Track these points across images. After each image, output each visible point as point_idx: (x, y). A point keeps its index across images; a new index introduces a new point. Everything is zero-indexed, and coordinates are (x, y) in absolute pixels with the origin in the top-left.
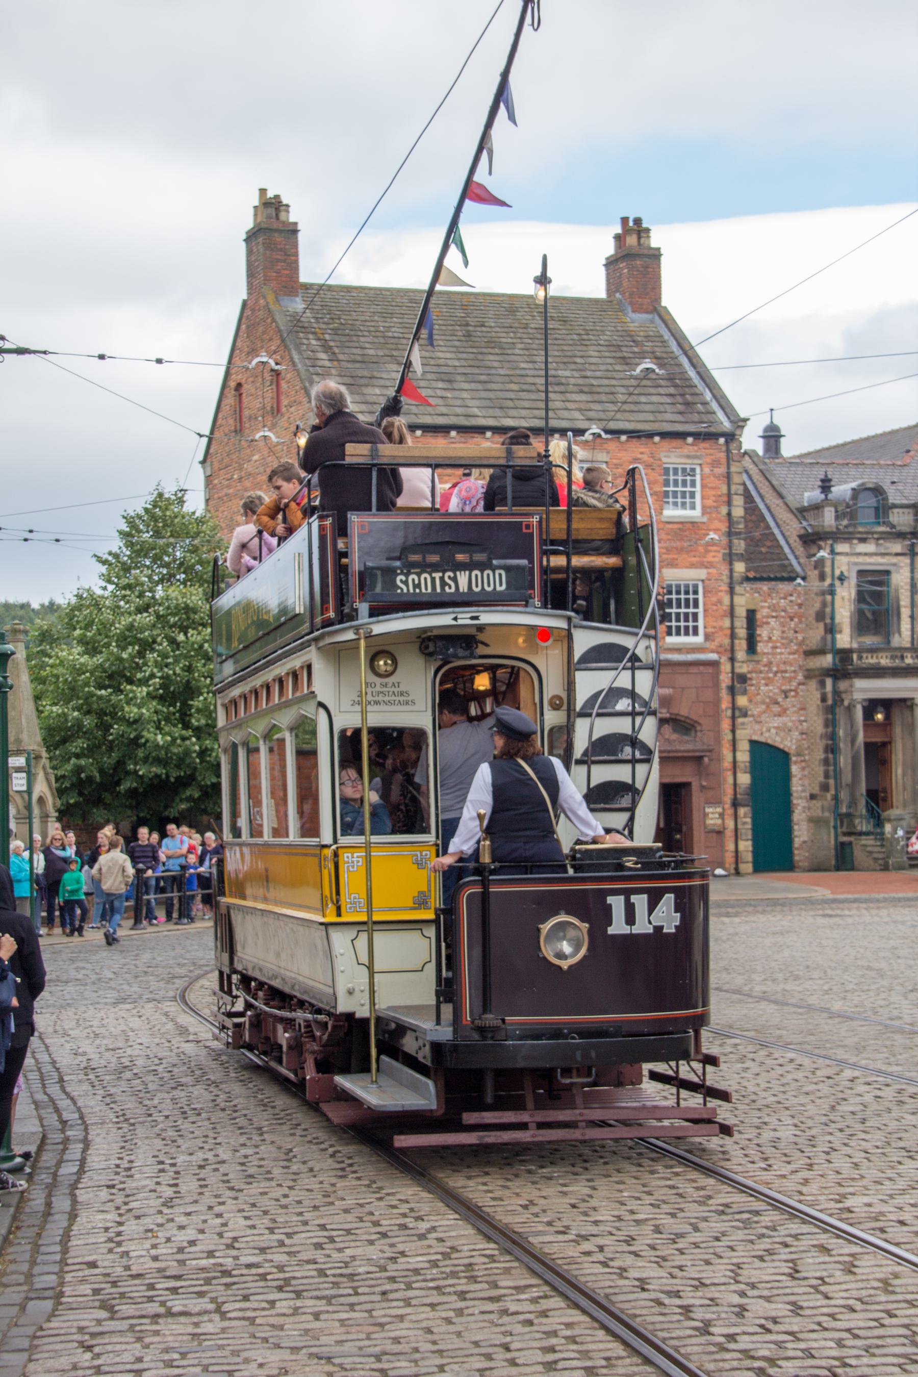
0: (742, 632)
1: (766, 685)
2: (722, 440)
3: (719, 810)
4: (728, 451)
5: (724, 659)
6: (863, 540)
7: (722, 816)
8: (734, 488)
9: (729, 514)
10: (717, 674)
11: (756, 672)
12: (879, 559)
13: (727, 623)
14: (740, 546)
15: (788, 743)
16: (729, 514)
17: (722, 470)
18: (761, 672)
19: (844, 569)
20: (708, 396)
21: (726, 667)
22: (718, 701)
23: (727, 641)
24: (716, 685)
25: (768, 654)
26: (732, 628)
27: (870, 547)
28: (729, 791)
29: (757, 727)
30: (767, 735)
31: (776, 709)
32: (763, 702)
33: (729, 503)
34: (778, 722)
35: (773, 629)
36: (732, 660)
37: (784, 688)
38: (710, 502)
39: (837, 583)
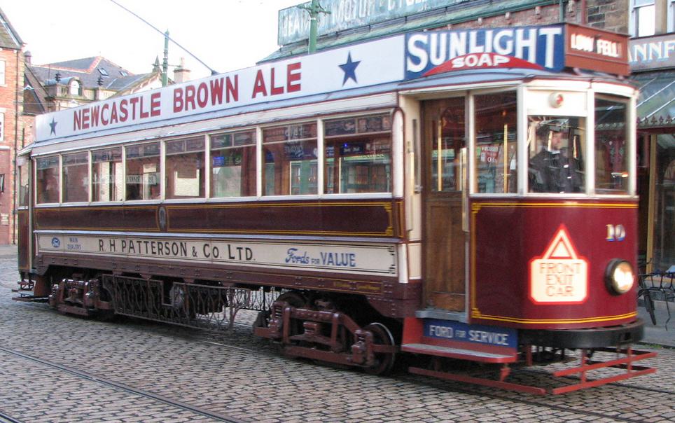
0: (20, 137)
2: (15, 51)
3: (7, 215)
4: (17, 56)
5: (12, 149)
7: (8, 218)
8: (19, 73)
9: (17, 85)
10: (9, 154)
13: (14, 132)
14: (21, 99)
16: (17, 85)
17: (15, 65)
20: (9, 32)
21: (13, 152)
22: (9, 166)
23: (14, 141)
24: (9, 161)
26: (16, 135)
28: (12, 207)
33: (17, 79)
36: (16, 149)
38: (9, 78)
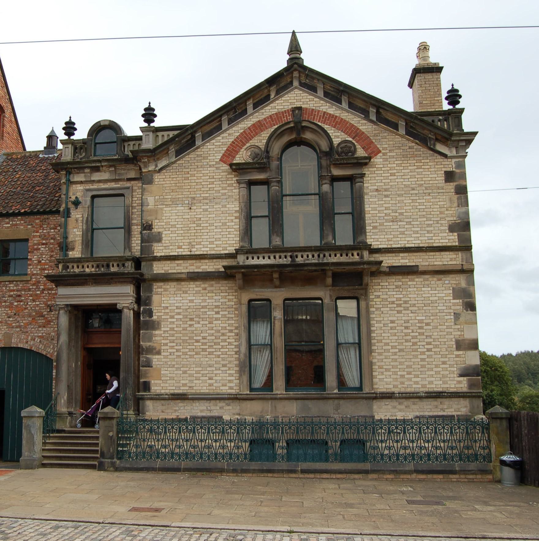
1: (34, 301)
6: (96, 169)
11: (25, 290)
12: (113, 185)
15: (49, 351)
18: (30, 290)
19: (79, 195)
25: (37, 274)
27: (104, 175)
29: (23, 336)
30: (32, 343)
31: (41, 321)
32: (30, 315)
34: (42, 331)
35: (42, 254)
37: (49, 303)
39: (71, 206)
